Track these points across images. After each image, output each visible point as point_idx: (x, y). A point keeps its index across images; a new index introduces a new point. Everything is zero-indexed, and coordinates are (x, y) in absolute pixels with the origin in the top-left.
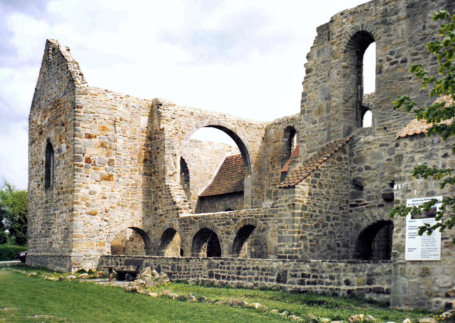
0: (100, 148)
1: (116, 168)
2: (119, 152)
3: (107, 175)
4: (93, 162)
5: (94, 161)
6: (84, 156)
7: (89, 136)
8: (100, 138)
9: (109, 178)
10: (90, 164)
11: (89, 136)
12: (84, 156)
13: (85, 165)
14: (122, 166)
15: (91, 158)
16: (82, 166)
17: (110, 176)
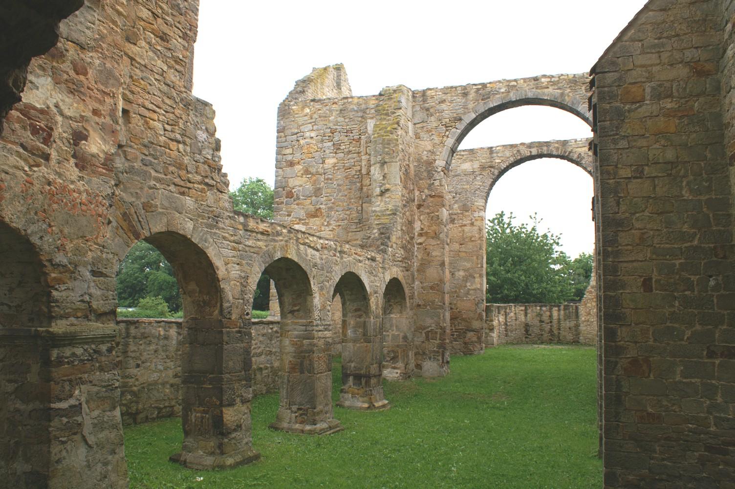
0: (304, 176)
1: (325, 198)
2: (330, 176)
3: (313, 210)
4: (295, 196)
5: (297, 194)
6: (284, 190)
7: (291, 162)
8: (304, 163)
9: (316, 214)
10: (292, 199)
11: (291, 162)
12: (284, 190)
13: (286, 201)
14: (335, 194)
15: (293, 191)
16: (282, 203)
17: (317, 210)
